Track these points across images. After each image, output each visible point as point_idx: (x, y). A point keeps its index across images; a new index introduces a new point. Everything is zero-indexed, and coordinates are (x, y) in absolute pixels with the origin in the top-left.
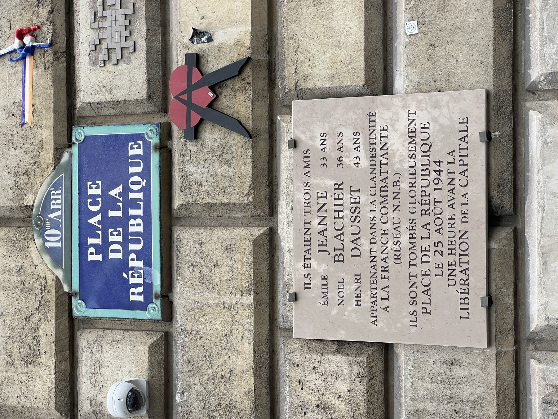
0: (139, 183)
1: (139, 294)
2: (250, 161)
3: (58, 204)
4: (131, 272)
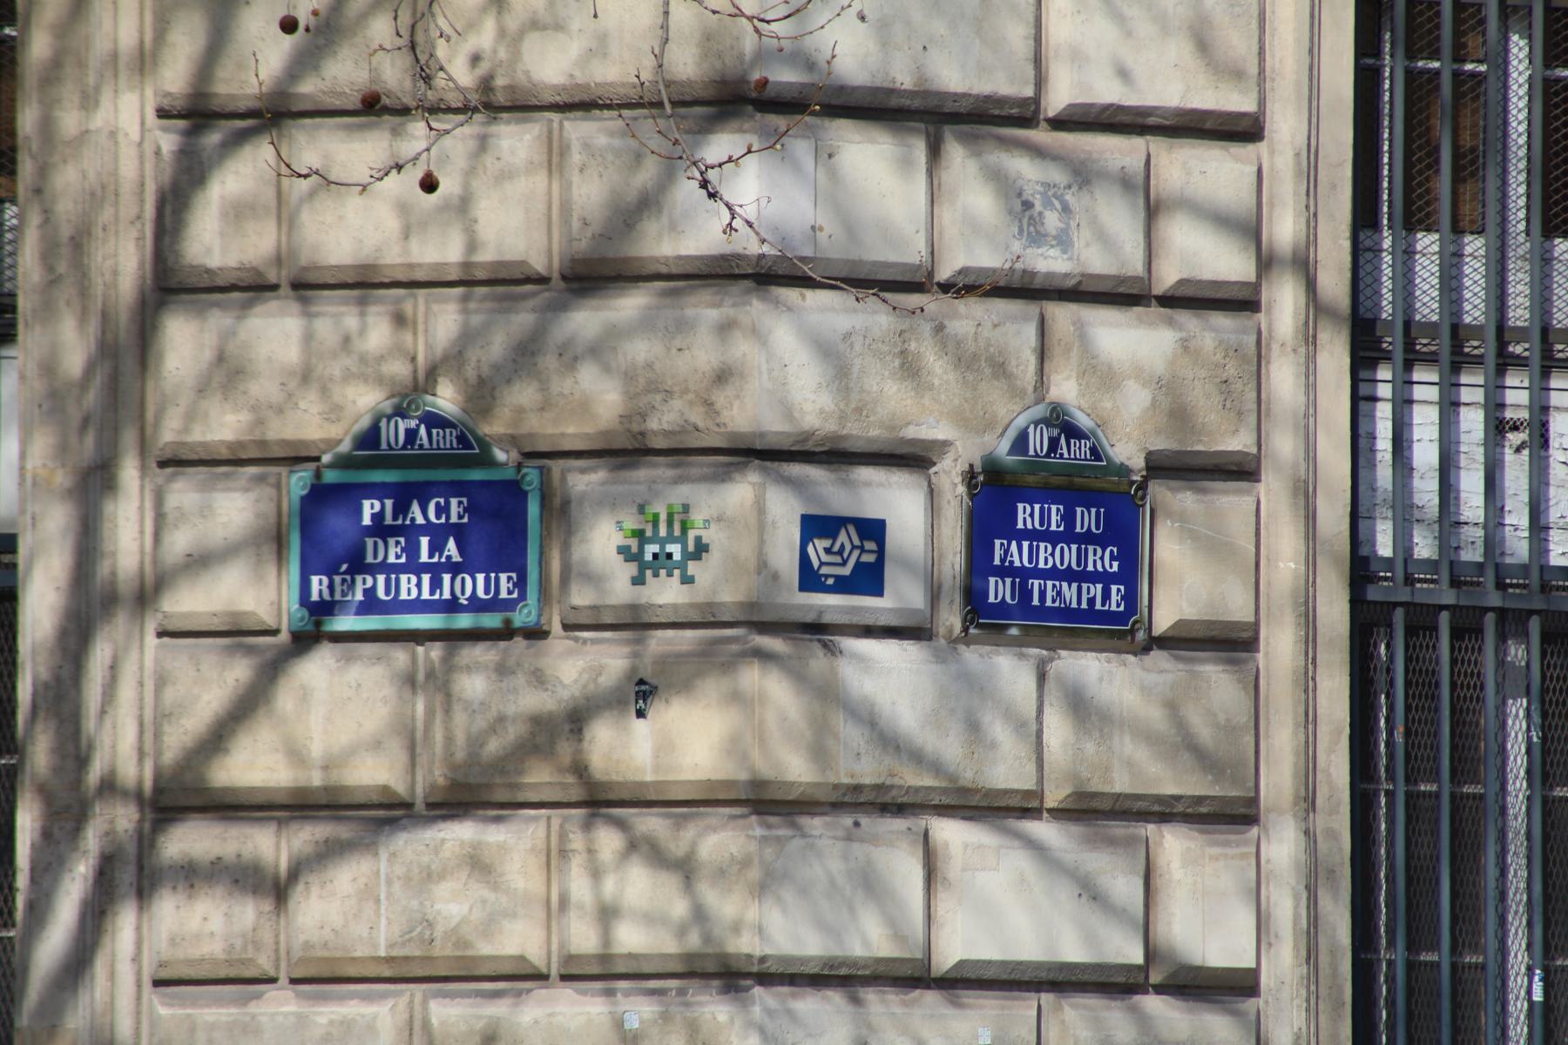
0: (463, 593)
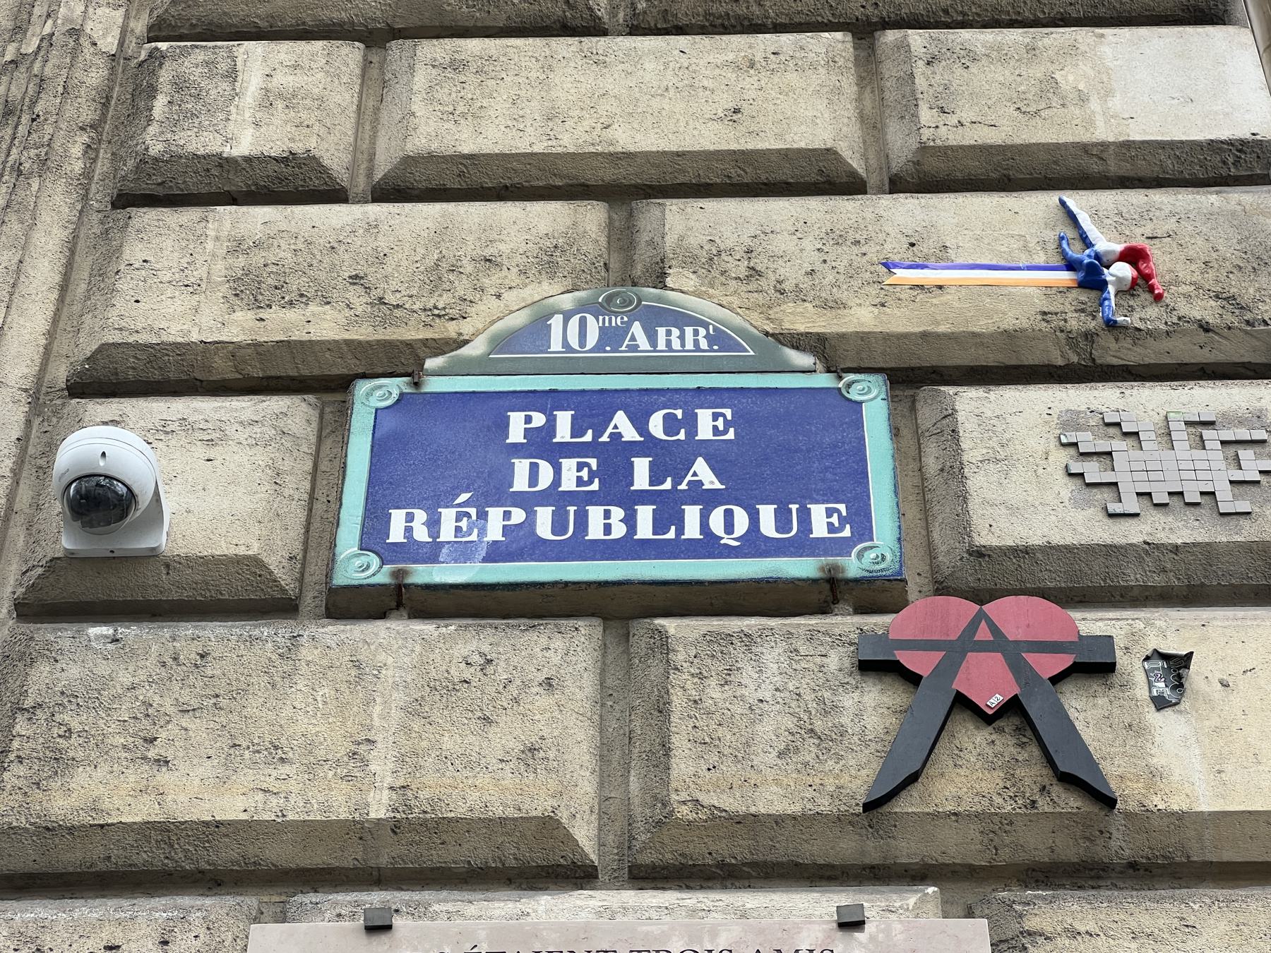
0: (729, 527)
1: (409, 530)
2: (796, 808)
3: (669, 343)
4: (473, 511)
